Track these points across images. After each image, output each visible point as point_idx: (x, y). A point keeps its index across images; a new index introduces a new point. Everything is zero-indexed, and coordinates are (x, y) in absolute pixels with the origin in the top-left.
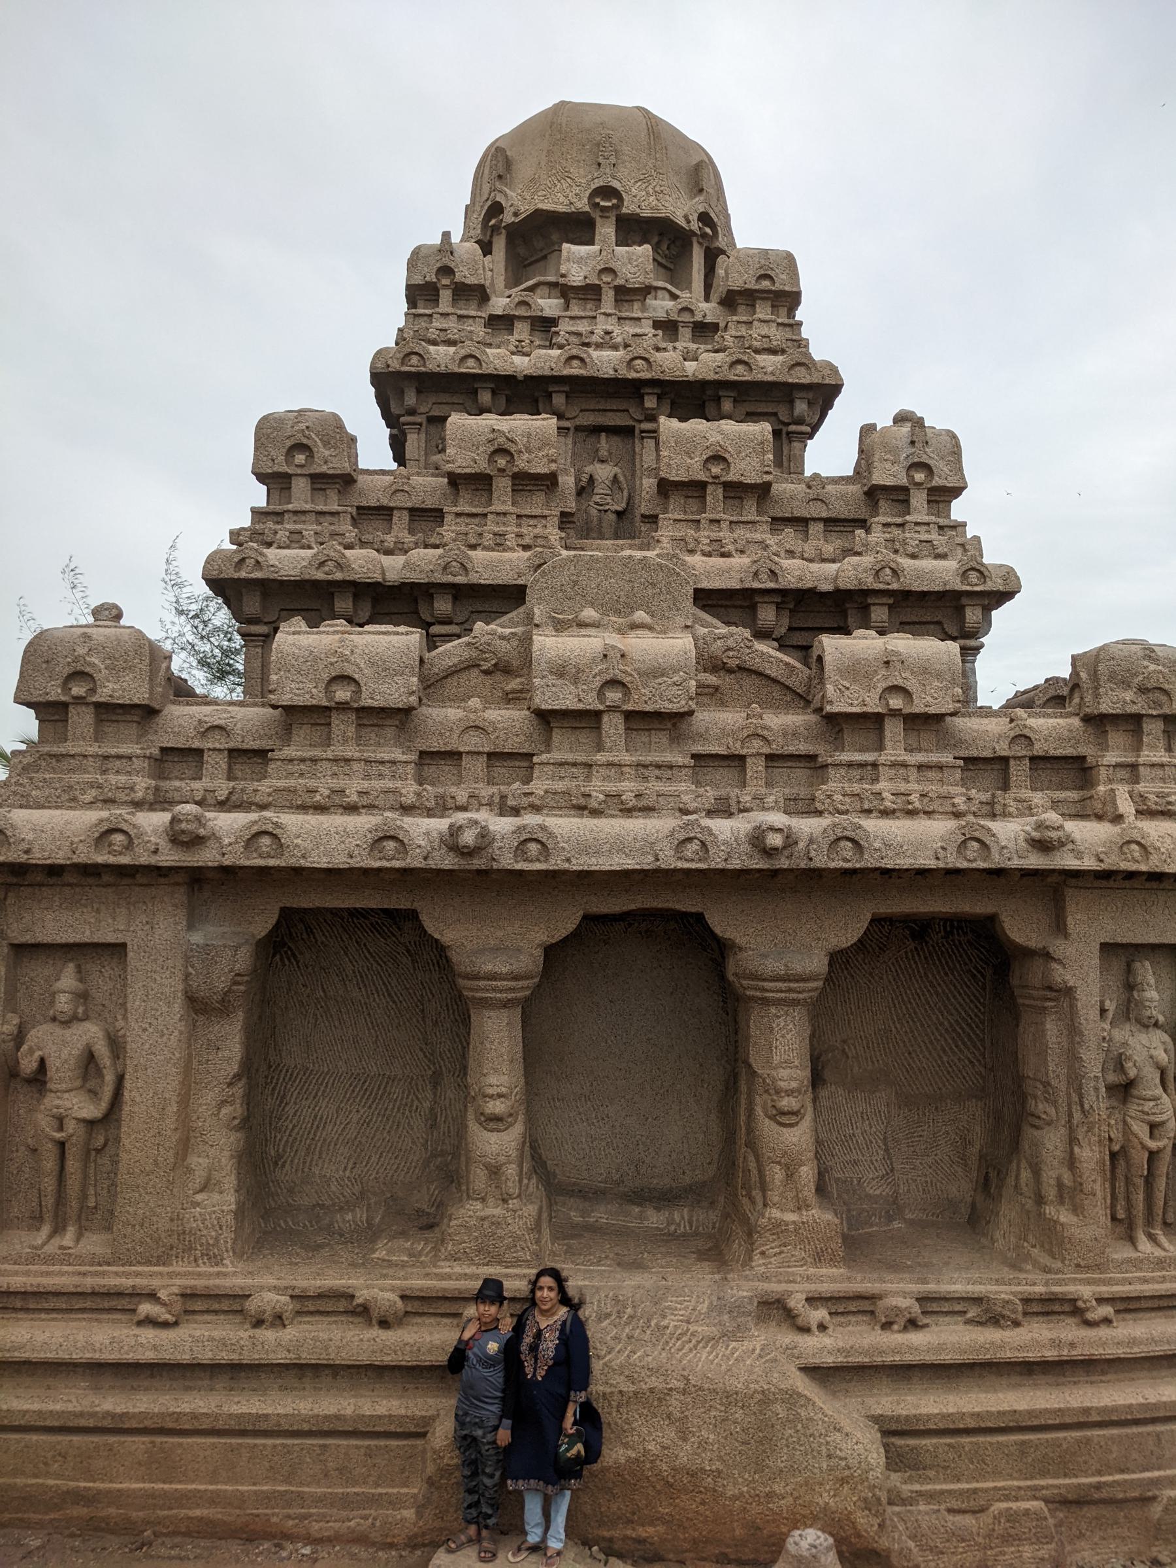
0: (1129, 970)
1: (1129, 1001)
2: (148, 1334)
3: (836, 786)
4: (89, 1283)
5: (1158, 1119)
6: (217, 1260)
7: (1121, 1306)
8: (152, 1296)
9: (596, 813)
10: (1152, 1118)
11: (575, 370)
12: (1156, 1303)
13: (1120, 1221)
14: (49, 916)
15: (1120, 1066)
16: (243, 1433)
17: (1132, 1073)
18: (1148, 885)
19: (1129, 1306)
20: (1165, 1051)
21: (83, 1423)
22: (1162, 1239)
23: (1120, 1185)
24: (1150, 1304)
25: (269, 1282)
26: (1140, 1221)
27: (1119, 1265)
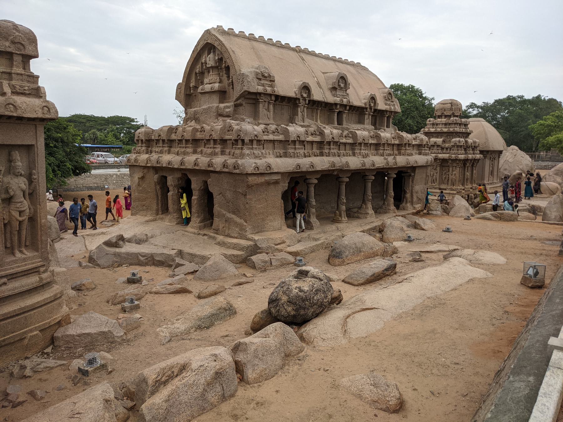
0: (10, 155)
1: (10, 167)
5: (23, 209)
7: (9, 277)
10: (20, 209)
12: (23, 273)
13: (8, 248)
15: (7, 191)
17: (12, 193)
18: (17, 122)
19: (13, 277)
20: (25, 184)
22: (25, 251)
23: (8, 235)
24: (21, 275)
26: (16, 247)
27: (9, 263)
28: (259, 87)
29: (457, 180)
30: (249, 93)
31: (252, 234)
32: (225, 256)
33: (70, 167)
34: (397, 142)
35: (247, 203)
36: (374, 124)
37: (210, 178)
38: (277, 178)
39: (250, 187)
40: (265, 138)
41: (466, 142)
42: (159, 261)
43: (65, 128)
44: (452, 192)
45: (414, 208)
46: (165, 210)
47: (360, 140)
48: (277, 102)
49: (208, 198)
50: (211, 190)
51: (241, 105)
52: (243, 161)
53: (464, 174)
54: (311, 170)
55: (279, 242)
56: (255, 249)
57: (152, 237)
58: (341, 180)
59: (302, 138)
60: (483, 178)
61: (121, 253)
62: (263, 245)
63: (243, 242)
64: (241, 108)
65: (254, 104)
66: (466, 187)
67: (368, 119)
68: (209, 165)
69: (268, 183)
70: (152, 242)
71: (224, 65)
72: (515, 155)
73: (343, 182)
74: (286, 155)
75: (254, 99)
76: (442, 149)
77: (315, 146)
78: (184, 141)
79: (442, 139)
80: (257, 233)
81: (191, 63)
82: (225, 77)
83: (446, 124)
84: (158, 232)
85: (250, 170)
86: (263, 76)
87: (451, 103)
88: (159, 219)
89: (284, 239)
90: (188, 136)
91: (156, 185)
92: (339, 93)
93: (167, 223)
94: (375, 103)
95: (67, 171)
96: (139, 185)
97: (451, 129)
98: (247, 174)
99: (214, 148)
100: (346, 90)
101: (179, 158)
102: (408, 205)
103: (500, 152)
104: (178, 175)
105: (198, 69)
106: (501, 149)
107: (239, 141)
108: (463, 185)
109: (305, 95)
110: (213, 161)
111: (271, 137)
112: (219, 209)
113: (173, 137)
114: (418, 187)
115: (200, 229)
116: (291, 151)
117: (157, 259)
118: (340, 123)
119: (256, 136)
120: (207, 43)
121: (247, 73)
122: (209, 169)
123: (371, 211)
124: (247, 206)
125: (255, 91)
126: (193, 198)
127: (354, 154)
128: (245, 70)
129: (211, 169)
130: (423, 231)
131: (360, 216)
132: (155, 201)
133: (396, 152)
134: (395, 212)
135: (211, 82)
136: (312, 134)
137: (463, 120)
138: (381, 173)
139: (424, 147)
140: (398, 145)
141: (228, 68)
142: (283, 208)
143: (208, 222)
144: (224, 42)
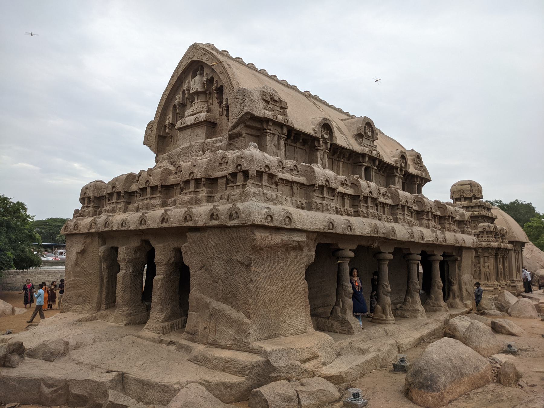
28: (267, 112)
29: (493, 272)
31: (259, 340)
32: (207, 385)
33: (12, 256)
35: (251, 280)
37: (186, 241)
38: (300, 240)
39: (256, 250)
40: (280, 175)
41: (495, 228)
42: (78, 396)
43: (15, 212)
44: (487, 288)
45: (466, 306)
46: (111, 302)
47: (403, 202)
48: (289, 141)
49: (181, 275)
50: (186, 261)
51: (239, 135)
52: (246, 204)
53: (497, 267)
54: (348, 233)
55: (308, 356)
56: (266, 373)
57: (76, 347)
58: (381, 256)
60: (511, 274)
61: (8, 378)
62: (280, 363)
63: (243, 357)
64: (239, 140)
65: (258, 136)
66: (502, 282)
68: (186, 218)
69: (286, 248)
70: (75, 357)
71: (215, 85)
72: (532, 251)
73: (384, 260)
74: (309, 207)
75: (258, 129)
77: (347, 201)
78: (148, 190)
80: (267, 338)
81: (167, 93)
82: (216, 107)
83: (467, 208)
84: (89, 338)
85: (259, 219)
87: (470, 184)
88: (100, 317)
89: (315, 350)
90: (154, 181)
91: (101, 262)
93: (113, 322)
94: (406, 163)
95: (6, 261)
96: (76, 264)
97: (476, 213)
99: (196, 192)
100: (373, 141)
101: (137, 215)
104: (135, 243)
105: (178, 99)
106: (525, 241)
107: (240, 175)
108: (497, 280)
109: (326, 136)
110: (194, 210)
111: (288, 176)
112: (198, 295)
113: (134, 187)
114: (466, 277)
115: (164, 333)
116: (319, 201)
117: (75, 391)
119: (267, 166)
120: (193, 62)
121: (249, 90)
123: (421, 308)
124: (251, 286)
125: (260, 115)
126: (156, 278)
127: (396, 220)
129: (190, 224)
130: (514, 337)
131: (406, 314)
132: (98, 288)
134: (446, 311)
135: (196, 112)
136: (342, 184)
138: (427, 253)
139: (466, 225)
140: (440, 217)
141: (220, 90)
142: (307, 295)
143: (179, 320)
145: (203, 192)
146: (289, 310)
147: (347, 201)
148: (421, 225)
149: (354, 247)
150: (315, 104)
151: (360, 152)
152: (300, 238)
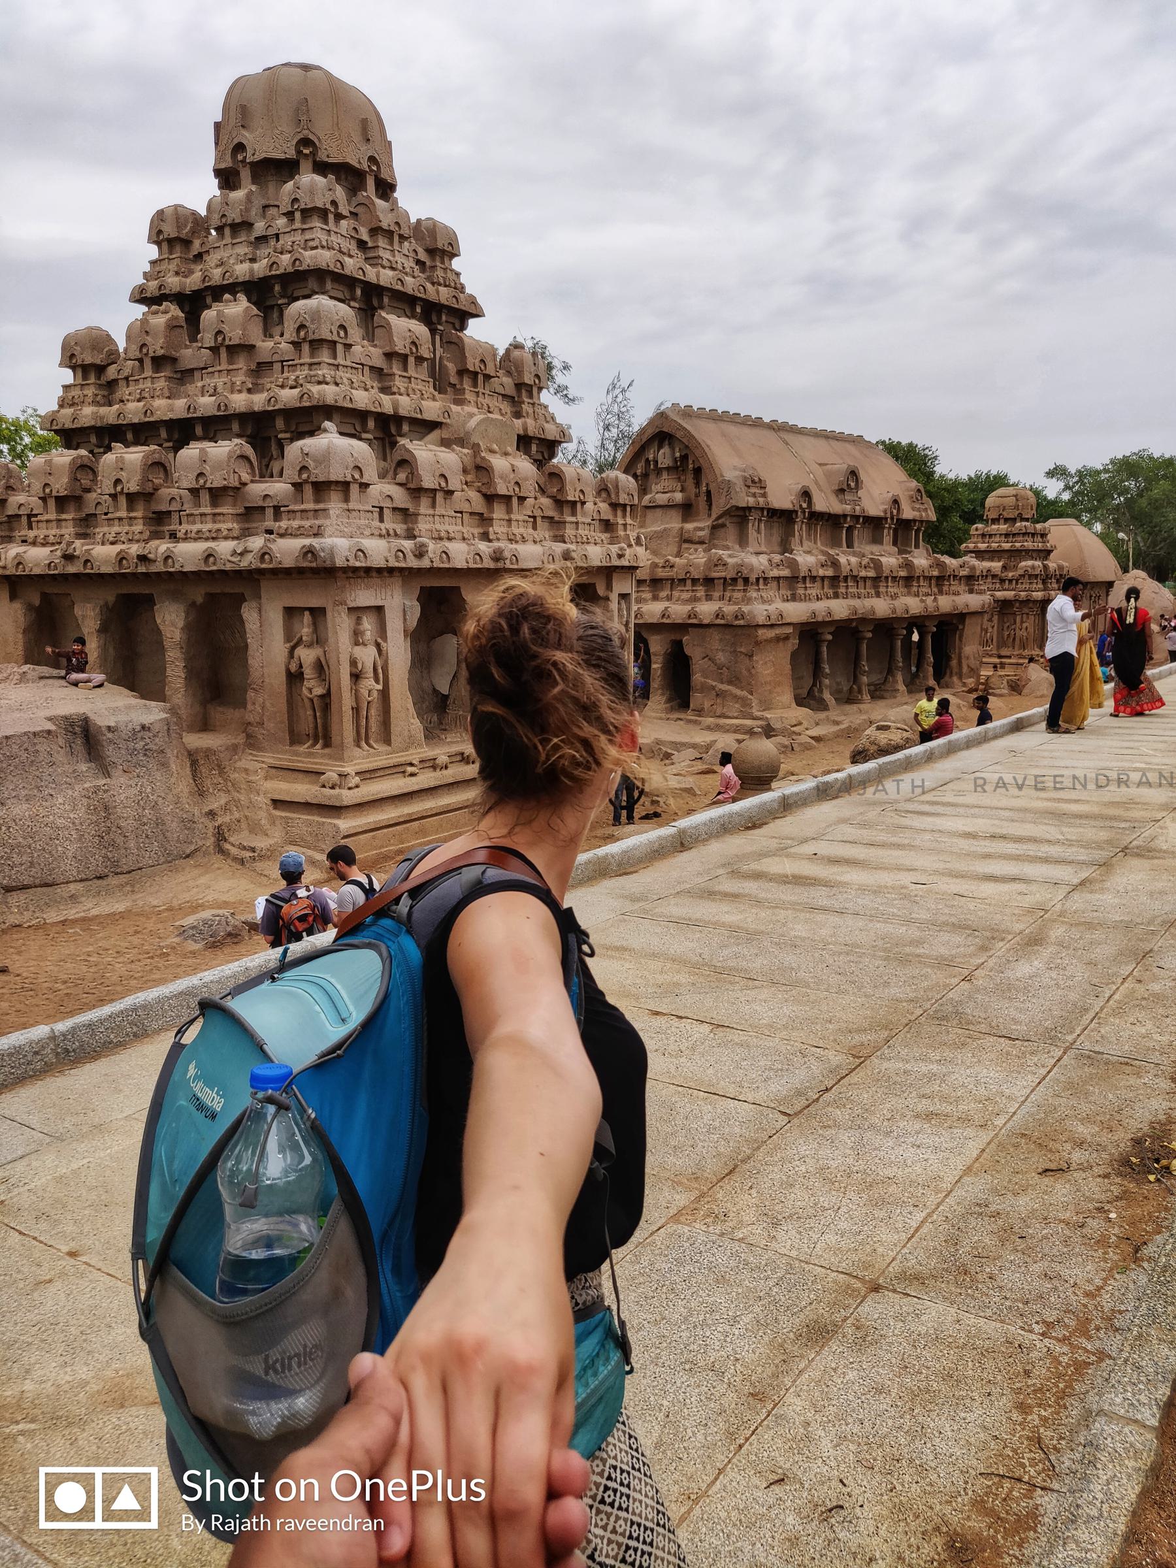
2: (413, 779)
3: (569, 531)
4: (392, 762)
6: (420, 745)
8: (411, 765)
9: (517, 542)
11: (399, 287)
14: (360, 593)
16: (436, 815)
21: (401, 820)
25: (441, 753)
30: (738, 508)
34: (936, 573)
36: (895, 543)
41: (1045, 567)
45: (964, 684)
47: (886, 573)
50: (688, 651)
51: (723, 526)
52: (749, 607)
59: (814, 574)
62: (776, 725)
64: (723, 530)
67: (888, 536)
73: (864, 638)
74: (794, 598)
76: (1002, 581)
79: (1000, 564)
83: (1007, 535)
85: (761, 620)
86: (753, 481)
87: (1015, 496)
92: (848, 496)
97: (1018, 545)
98: (758, 626)
102: (955, 679)
103: (1110, 584)
107: (742, 580)
109: (805, 505)
116: (801, 591)
118: (850, 545)
120: (661, 432)
121: (734, 480)
122: (691, 621)
123: (902, 687)
124: (753, 671)
127: (878, 595)
128: (730, 474)
131: (885, 694)
133: (935, 590)
137: (1039, 526)
140: (938, 578)
141: (698, 471)
144: (693, 432)
145: (701, 592)
146: (778, 689)
147: (826, 582)
148: (909, 594)
149: (832, 629)
150: (787, 444)
151: (840, 512)
152: (790, 630)
